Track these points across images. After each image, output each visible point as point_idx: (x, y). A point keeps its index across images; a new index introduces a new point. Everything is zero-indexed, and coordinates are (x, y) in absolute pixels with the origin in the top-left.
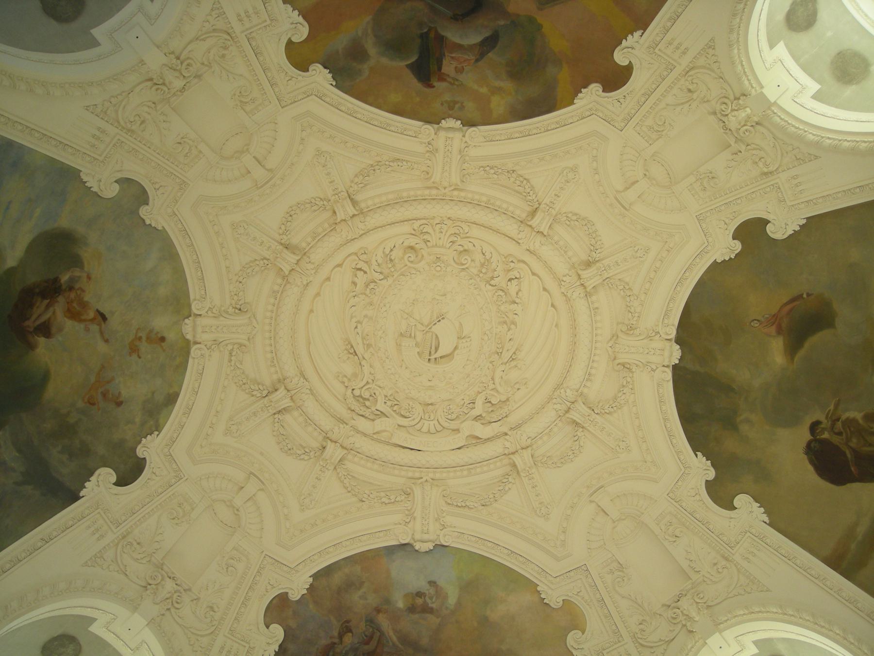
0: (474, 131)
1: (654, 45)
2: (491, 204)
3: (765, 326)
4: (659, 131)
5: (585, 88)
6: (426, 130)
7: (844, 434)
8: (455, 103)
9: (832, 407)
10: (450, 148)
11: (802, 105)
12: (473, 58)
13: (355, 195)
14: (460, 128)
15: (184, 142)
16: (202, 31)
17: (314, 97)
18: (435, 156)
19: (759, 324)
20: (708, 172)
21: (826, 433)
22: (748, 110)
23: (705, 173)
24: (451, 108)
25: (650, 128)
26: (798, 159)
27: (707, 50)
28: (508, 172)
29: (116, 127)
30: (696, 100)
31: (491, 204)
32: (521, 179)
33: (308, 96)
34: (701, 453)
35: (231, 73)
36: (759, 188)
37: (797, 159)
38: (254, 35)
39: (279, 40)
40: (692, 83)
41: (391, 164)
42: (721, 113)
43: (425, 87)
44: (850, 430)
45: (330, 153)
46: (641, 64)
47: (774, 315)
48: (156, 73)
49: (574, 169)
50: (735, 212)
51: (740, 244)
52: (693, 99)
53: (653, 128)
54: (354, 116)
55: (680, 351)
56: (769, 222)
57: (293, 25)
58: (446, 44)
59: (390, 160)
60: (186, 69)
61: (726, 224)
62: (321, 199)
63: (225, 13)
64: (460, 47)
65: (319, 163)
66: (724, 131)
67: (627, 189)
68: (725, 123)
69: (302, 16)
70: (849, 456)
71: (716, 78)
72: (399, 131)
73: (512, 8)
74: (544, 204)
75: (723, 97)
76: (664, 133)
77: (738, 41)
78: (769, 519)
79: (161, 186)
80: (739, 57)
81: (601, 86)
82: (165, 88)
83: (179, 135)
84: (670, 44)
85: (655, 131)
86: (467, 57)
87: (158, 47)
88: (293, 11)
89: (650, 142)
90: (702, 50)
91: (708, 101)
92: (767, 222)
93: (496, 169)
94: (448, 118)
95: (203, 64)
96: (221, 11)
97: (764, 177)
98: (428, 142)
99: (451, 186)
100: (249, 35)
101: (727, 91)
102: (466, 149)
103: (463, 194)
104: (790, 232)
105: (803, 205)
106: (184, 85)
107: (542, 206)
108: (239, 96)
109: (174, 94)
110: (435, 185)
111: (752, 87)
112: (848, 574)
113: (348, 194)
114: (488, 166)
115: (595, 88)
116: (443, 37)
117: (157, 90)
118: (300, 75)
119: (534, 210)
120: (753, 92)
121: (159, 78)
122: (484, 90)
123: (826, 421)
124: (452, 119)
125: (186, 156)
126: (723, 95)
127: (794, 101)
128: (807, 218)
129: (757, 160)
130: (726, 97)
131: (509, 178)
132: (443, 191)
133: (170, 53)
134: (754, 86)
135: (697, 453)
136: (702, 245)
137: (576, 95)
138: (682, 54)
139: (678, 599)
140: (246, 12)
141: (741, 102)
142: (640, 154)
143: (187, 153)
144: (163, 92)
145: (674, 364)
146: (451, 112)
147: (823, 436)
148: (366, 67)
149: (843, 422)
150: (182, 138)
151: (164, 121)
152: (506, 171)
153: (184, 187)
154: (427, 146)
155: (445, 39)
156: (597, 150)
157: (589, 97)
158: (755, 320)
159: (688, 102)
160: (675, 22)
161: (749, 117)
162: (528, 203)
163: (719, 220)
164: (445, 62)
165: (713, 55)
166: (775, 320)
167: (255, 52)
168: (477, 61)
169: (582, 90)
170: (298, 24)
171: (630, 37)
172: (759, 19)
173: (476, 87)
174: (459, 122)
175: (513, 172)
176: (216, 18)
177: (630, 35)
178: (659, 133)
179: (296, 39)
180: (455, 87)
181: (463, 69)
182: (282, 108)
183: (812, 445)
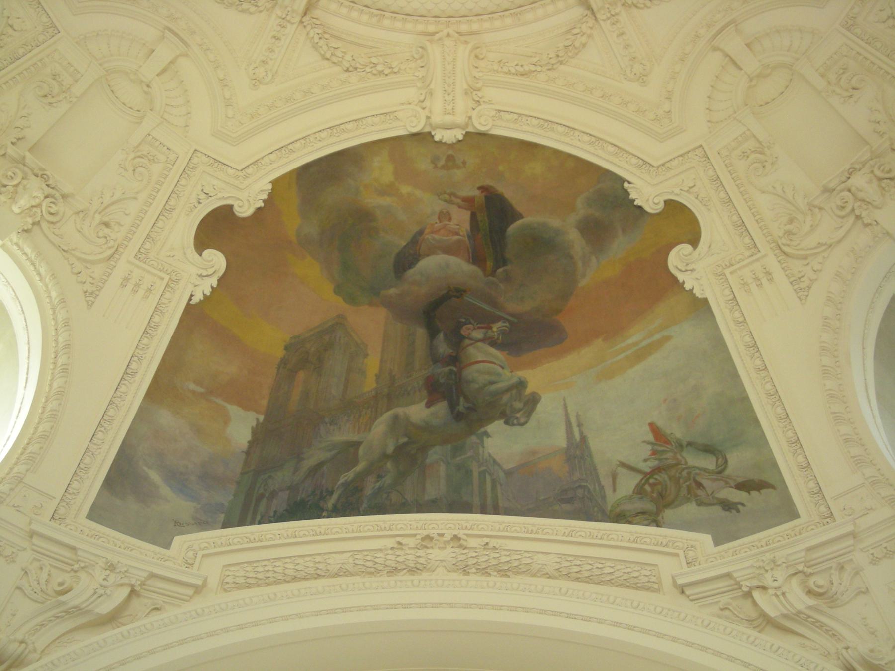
0: (413, 127)
1: (172, 285)
2: (377, 16)
4: (139, 157)
5: (259, 209)
6: (485, 124)
8: (444, 167)
10: (447, 98)
12: (428, 236)
13: (585, 15)
14: (434, 130)
15: (847, 91)
16: (824, 258)
17: (655, 164)
18: (469, 85)
22: (16, 210)
23: (59, 101)
24: (450, 158)
25: (153, 159)
27: (95, 289)
28: (356, 68)
30: (95, 213)
31: (377, 16)
32: (334, 59)
33: (663, 165)
35: (779, 196)
38: (747, 253)
39: (710, 246)
40: (106, 237)
41: (532, 68)
42: (53, 197)
43: (491, 187)
45: (626, 78)
46: (185, 254)
48: (890, 195)
49: (256, 82)
52: (100, 213)
53: (149, 160)
54: (593, 138)
57: (691, 268)
59: (535, 73)
60: (846, 202)
61: (11, 26)
62: (636, 7)
63: (791, 283)
64: (448, 250)
65: (641, 63)
66: (45, 173)
67: (172, 62)
68: (47, 185)
71: (74, 250)
72: (524, 118)
73: (382, 313)
74: (294, 23)
75: (57, 222)
76: (132, 155)
77: (54, 309)
79: (884, 22)
80: (46, 286)
81: (236, 213)
82: (878, 173)
83: (855, 102)
84: (149, 290)
85: (147, 157)
86: (436, 236)
87: (888, 233)
88: (693, 289)
90: (102, 288)
91: (77, 213)
93: (375, 72)
94: (454, 143)
95: (821, 209)
96: (796, 287)
98: (480, 105)
99: (440, 39)
100: (755, 252)
101: (54, 233)
102: (422, 98)
103: (420, 28)
106: (849, 178)
107: (297, 19)
108: (766, 161)
109: (864, 164)
110: (463, 38)
111: (17, 244)
113: (595, 17)
114: (387, 75)
115: (244, 210)
117: (889, 171)
118: (677, 195)
119: (308, 12)
120: (14, 237)
121: (886, 189)
122: (405, 189)
124: (448, 142)
125: (845, 69)
126: (58, 224)
130: (52, 223)
131: (354, 60)
132: (450, 31)
133: (870, 224)
134: (15, 247)
137: (270, 195)
138: (129, 277)
140: (760, 286)
141: (30, 220)
142: (161, 117)
143: (843, 73)
144: (882, 168)
146: (450, 152)
148: (581, 209)
150: (851, 97)
151: (878, 122)
152: (358, 70)
153: (849, 21)
154: (481, 98)
155: (471, 261)
156: (227, 117)
159: (106, 208)
160: (149, 322)
161: (14, 199)
162: (318, 22)
164: (466, 226)
165: (85, 283)
167: (744, 228)
168: (421, 232)
169: (262, 205)
170: (683, 270)
171: (208, 292)
172: (29, 344)
173: (418, 193)
174: (437, 138)
175: (348, 68)
176: (802, 277)
177: (208, 294)
178: (139, 154)
179: (685, 248)
180: (448, 191)
181: (439, 218)
182: (701, 146)
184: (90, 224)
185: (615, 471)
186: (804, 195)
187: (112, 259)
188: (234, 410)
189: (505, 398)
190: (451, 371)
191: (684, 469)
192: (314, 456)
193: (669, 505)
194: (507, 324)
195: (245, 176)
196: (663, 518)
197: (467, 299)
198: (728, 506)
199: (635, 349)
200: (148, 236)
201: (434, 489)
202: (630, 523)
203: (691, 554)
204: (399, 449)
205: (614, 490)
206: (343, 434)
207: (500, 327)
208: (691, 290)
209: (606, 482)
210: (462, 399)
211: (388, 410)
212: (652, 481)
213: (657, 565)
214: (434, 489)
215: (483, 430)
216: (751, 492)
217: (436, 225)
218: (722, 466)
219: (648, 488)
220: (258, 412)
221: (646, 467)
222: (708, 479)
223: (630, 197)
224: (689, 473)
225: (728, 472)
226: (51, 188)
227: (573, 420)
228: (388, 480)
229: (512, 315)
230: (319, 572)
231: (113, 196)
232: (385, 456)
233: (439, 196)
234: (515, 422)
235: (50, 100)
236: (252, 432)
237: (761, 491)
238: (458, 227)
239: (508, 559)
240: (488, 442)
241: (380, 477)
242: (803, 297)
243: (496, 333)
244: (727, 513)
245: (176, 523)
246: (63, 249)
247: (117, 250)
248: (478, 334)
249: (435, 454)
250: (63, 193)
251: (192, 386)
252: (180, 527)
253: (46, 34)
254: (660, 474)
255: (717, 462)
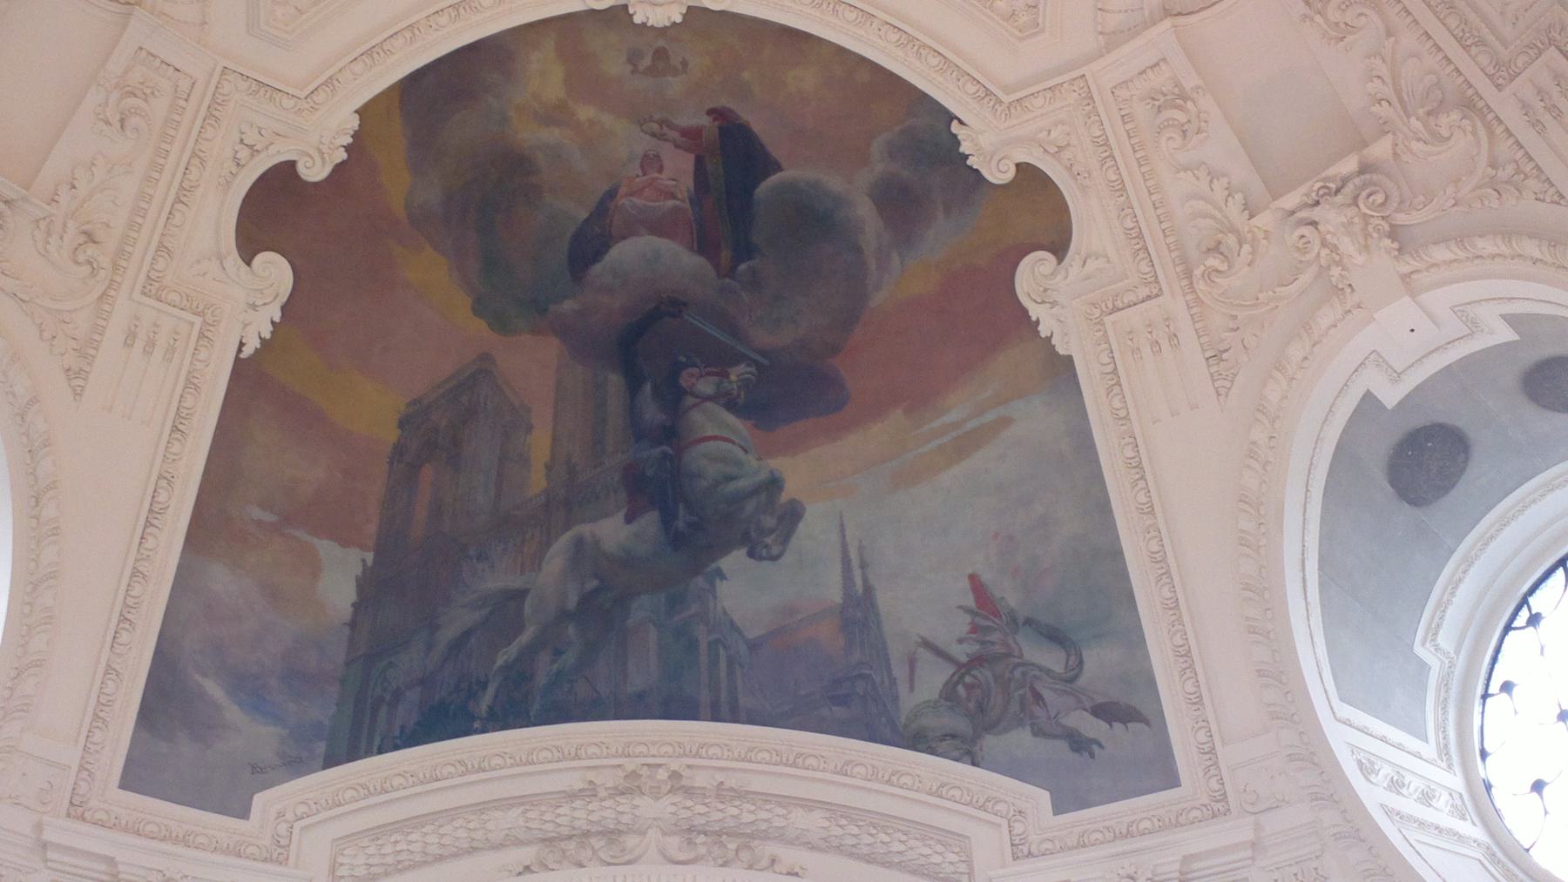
12: (624, 201)
17: (1006, 99)
24: (660, 54)
29: (1501, 122)
43: (731, 111)
58: (692, 233)
64: (658, 227)
69: (1030, 317)
73: (550, 349)
86: (637, 201)
88: (1052, 336)
89: (144, 53)
94: (665, 29)
115: (314, 171)
116: (701, 251)
122: (585, 112)
146: (661, 43)
150: (1342, 39)
157: (323, 140)
164: (687, 183)
168: (611, 194)
169: (344, 156)
170: (1039, 301)
173: (607, 119)
174: (638, 19)
177: (267, 336)
180: (657, 117)
185: (914, 653)
186: (1244, 205)
188: (326, 548)
189: (750, 506)
190: (665, 454)
191: (1019, 665)
192: (458, 619)
193: (991, 727)
194: (753, 369)
195: (312, 107)
196: (981, 750)
197: (690, 319)
198: (1079, 743)
199: (954, 434)
200: (161, 246)
201: (641, 675)
202: (932, 751)
203: (1018, 828)
204: (586, 600)
205: (912, 688)
206: (497, 579)
207: (742, 374)
208: (1049, 339)
209: (900, 672)
210: (681, 507)
211: (567, 528)
212: (968, 679)
213: (968, 837)
214: (641, 675)
215: (714, 566)
216: (1114, 724)
217: (637, 180)
218: (1073, 670)
219: (961, 690)
220: (362, 547)
221: (962, 652)
222: (1051, 689)
223: (961, 150)
224: (1024, 674)
225: (1082, 681)
227: (853, 555)
228: (570, 658)
229: (763, 353)
230: (475, 844)
232: (564, 616)
233: (641, 125)
234: (764, 552)
236: (357, 586)
237: (1129, 725)
238: (674, 183)
239: (752, 818)
240: (722, 588)
241: (558, 653)
242: (1222, 391)
243: (735, 387)
244: (1077, 756)
245: (255, 769)
248: (706, 386)
249: (642, 609)
251: (257, 513)
252: (263, 774)
254: (981, 669)
255: (1067, 663)
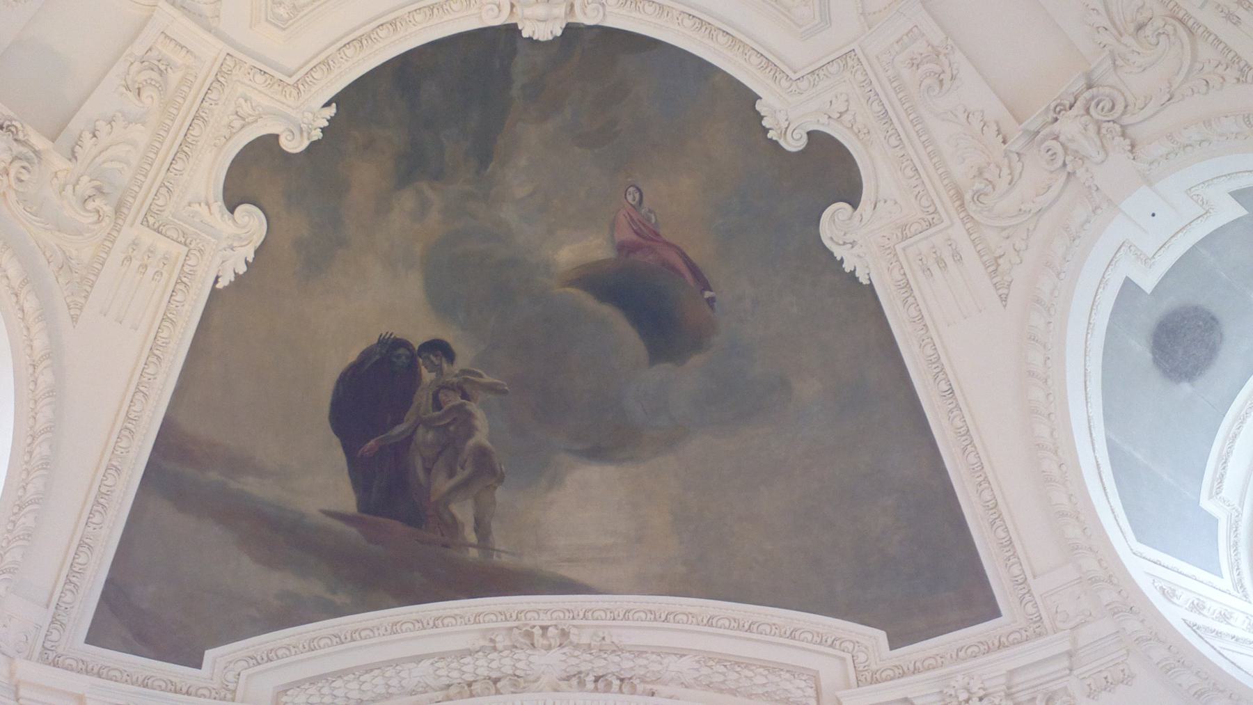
3: (631, 217)
7: (437, 413)
9: (487, 379)
11: (1113, 263)
19: (633, 203)
20: (955, 73)
21: (433, 375)
26: (996, 261)
30: (1119, 41)
34: (336, 114)
36: (929, 187)
37: (996, 259)
40: (1159, 34)
44: (449, 424)
47: (657, 234)
50: (869, 132)
51: (800, 149)
52: (1121, 35)
55: (550, 38)
56: (855, 206)
61: (841, 114)
70: (399, 429)
78: (225, 287)
92: (855, 204)
97: (952, 192)
104: (838, 252)
105: (900, 277)
112: (154, 478)
123: (457, 372)
127: (1120, 248)
128: (871, 285)
129: (986, 175)
135: (334, 105)
136: (791, 68)
139: (5, 126)
145: (520, 28)
147: (424, 371)
149: (461, 406)
158: (641, 195)
163: (847, 101)
165: (1223, 78)
166: (648, 237)
183: (401, 351)
184: (1135, 54)
187: (1194, 31)
226: (1075, 102)
231: (1097, 11)
235: (946, 77)
246: (1169, 100)
247: (1181, 21)
250: (1085, 86)
253: (855, 69)
